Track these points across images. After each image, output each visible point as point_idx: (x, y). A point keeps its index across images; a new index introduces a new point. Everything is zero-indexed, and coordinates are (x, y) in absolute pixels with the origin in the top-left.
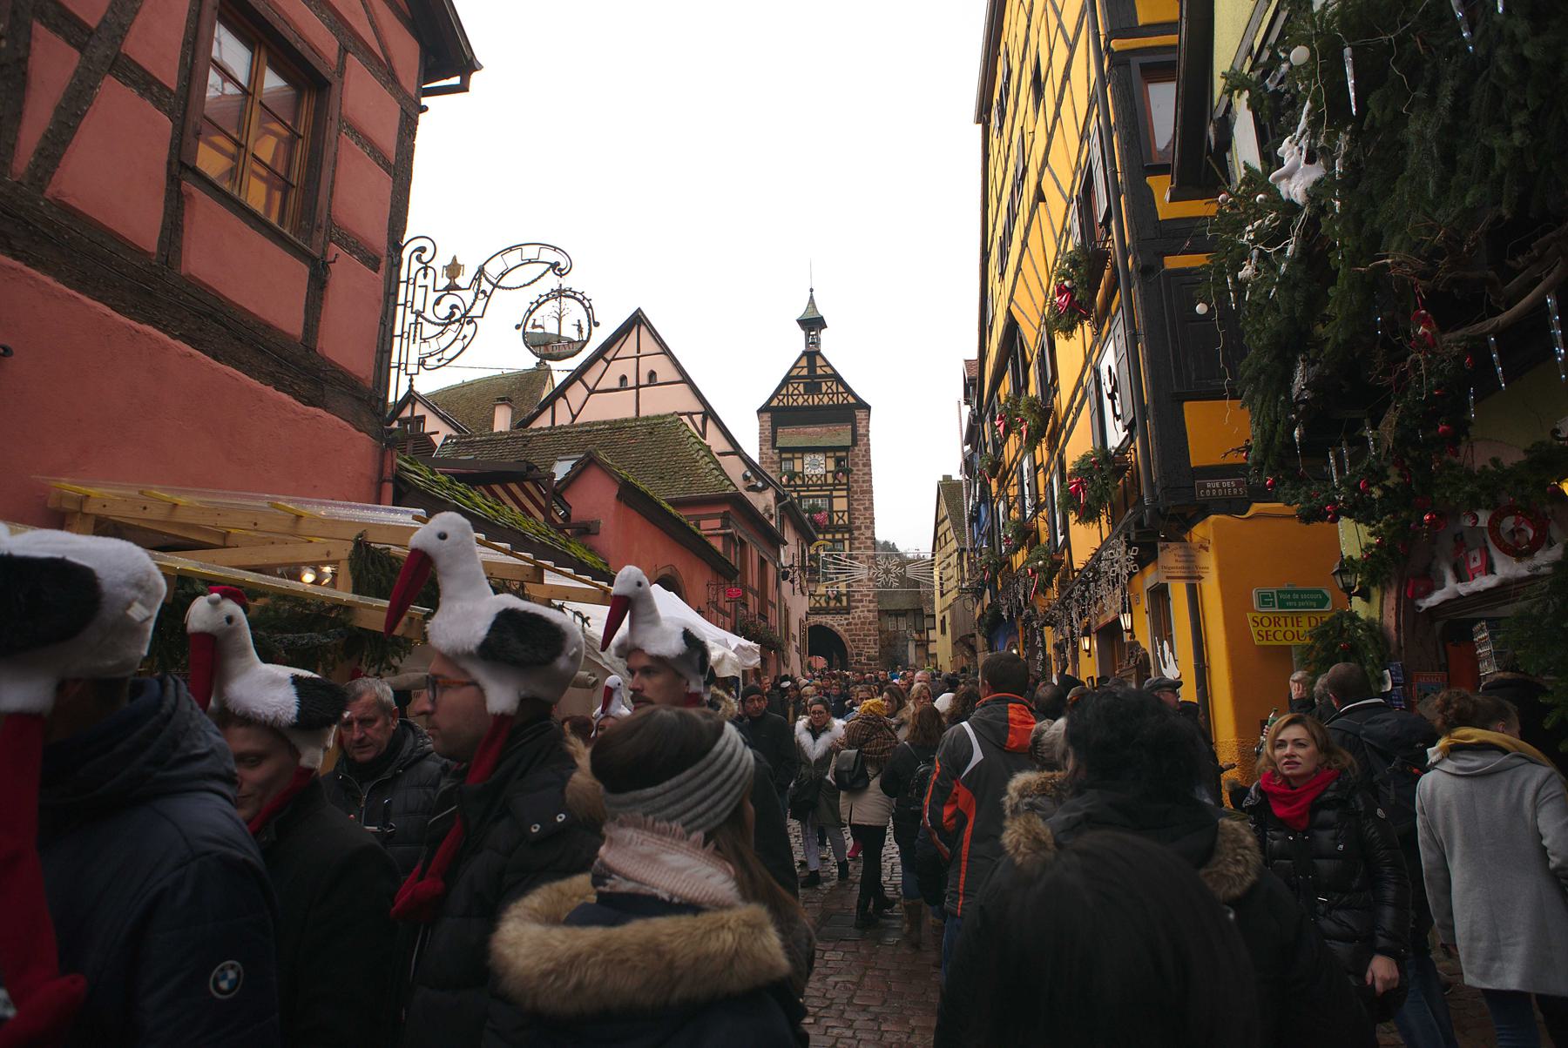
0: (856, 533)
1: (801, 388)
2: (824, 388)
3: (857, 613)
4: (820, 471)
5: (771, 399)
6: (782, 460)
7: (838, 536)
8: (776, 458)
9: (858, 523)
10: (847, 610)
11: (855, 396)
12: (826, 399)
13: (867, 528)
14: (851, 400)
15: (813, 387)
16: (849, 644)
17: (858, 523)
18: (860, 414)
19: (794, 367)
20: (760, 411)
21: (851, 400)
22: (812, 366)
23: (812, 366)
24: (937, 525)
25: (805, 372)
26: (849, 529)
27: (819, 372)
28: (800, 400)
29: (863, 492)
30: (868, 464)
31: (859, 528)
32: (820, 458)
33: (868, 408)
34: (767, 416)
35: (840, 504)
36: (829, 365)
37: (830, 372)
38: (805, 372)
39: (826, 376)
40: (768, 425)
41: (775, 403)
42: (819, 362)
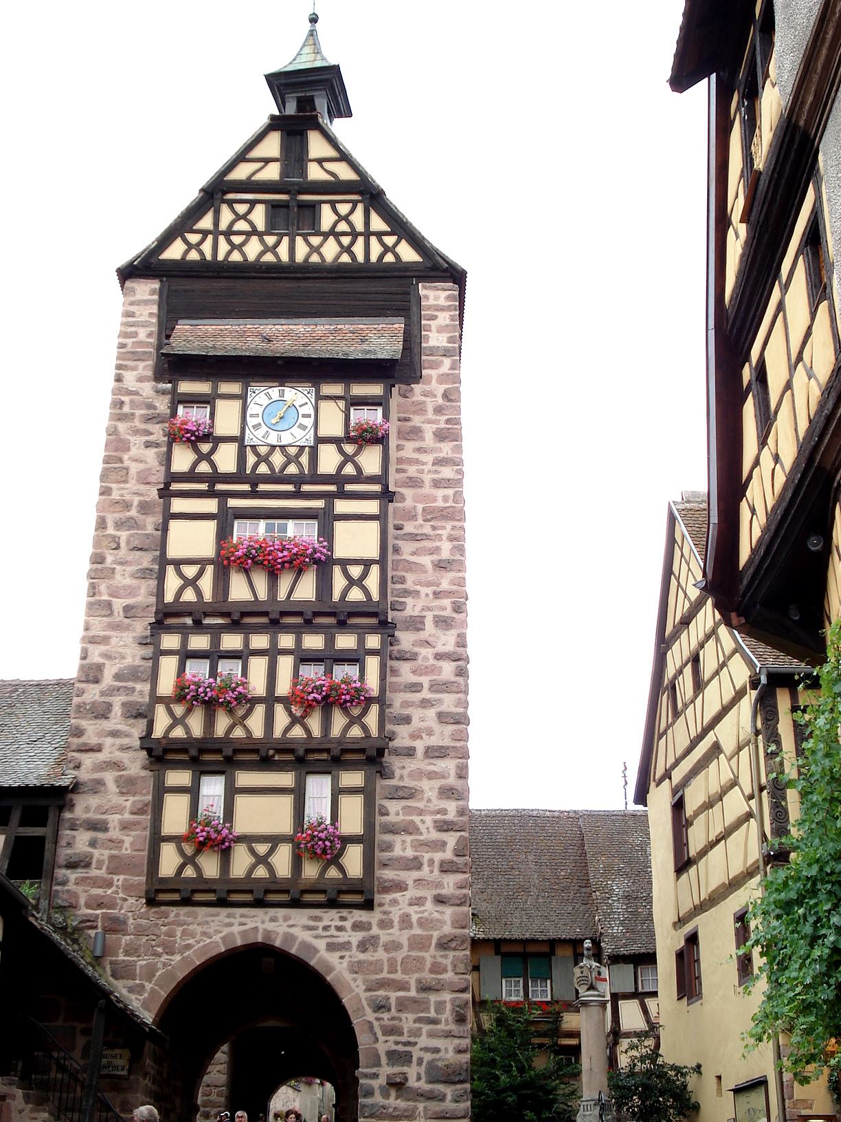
0: (406, 640)
1: (259, 216)
2: (327, 218)
3: (395, 905)
4: (298, 436)
5: (166, 240)
6: (181, 400)
7: (345, 641)
8: (162, 405)
10: (359, 896)
11: (417, 242)
12: (330, 250)
13: (443, 623)
14: (408, 254)
15: (294, 206)
16: (362, 1017)
17: (412, 607)
18: (434, 295)
19: (242, 157)
20: (128, 273)
21: (408, 254)
22: (294, 156)
23: (294, 156)
24: (664, 643)
25: (272, 173)
26: (378, 618)
28: (253, 249)
29: (434, 515)
30: (450, 434)
31: (416, 624)
32: (298, 396)
33: (456, 276)
34: (147, 289)
35: (356, 540)
36: (344, 157)
37: (345, 173)
39: (335, 187)
40: (148, 313)
41: (175, 251)
42: (317, 146)
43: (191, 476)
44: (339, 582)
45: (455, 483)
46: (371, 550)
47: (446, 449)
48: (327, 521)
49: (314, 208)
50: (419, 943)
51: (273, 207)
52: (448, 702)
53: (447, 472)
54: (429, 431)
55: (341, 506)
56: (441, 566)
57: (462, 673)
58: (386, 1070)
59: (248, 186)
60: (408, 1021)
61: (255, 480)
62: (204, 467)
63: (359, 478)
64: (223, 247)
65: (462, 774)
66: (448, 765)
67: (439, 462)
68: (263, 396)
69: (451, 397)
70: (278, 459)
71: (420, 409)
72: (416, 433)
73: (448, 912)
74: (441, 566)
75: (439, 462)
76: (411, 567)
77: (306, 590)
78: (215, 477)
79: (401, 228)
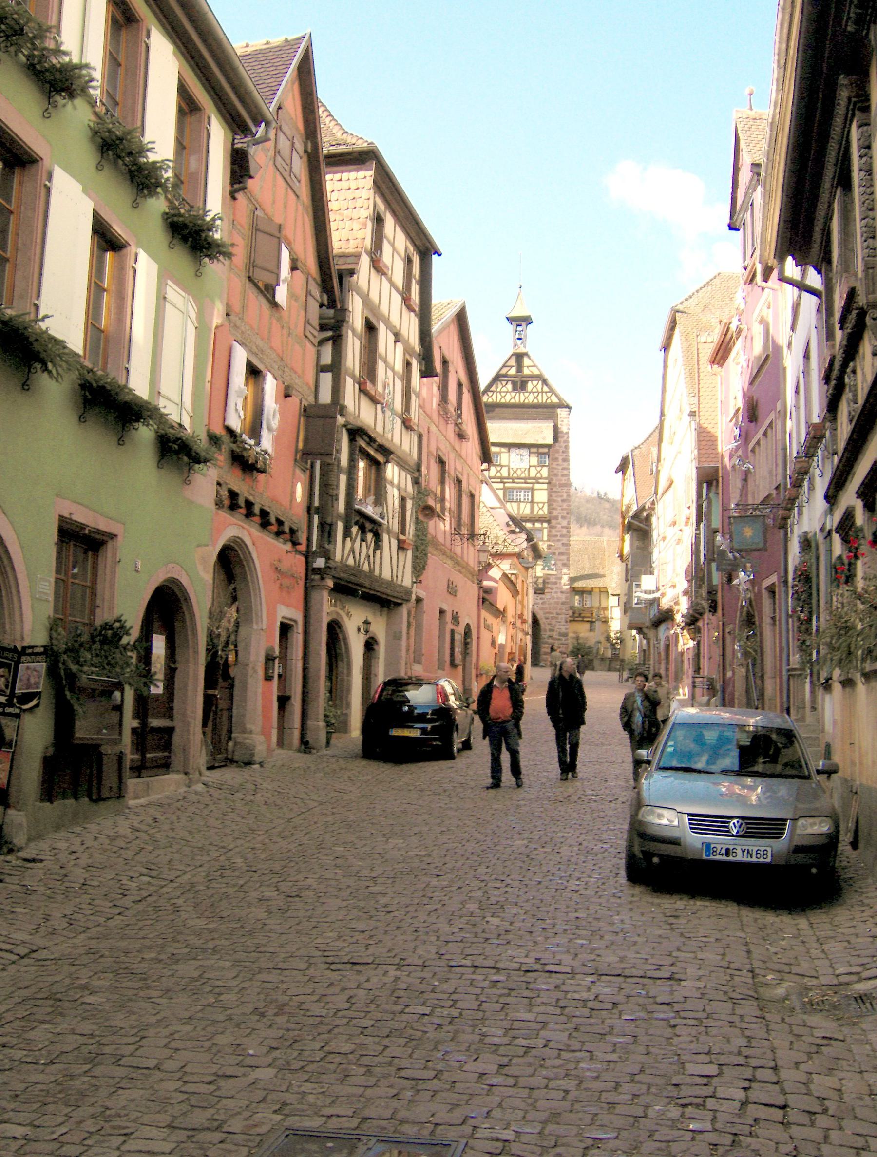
1: (509, 387)
2: (530, 386)
9: (555, 513)
13: (563, 518)
14: (555, 400)
15: (520, 385)
17: (555, 513)
18: (562, 413)
19: (504, 366)
23: (520, 368)
27: (526, 371)
29: (561, 485)
30: (566, 460)
31: (556, 518)
37: (536, 372)
38: (513, 371)
42: (526, 361)
43: (495, 478)
44: (536, 508)
45: (568, 475)
46: (545, 499)
47: (565, 465)
48: (533, 490)
49: (526, 382)
50: (557, 603)
51: (514, 384)
52: (565, 540)
53: (565, 472)
54: (560, 458)
55: (537, 486)
56: (563, 501)
57: (569, 532)
58: (548, 633)
59: (505, 376)
60: (553, 622)
61: (513, 479)
62: (499, 475)
63: (541, 478)
64: (499, 397)
65: (568, 560)
66: (564, 557)
67: (564, 469)
68: (514, 452)
69: (567, 447)
70: (519, 472)
71: (558, 451)
72: (556, 459)
73: (564, 596)
74: (563, 501)
75: (564, 469)
76: (555, 501)
77: (527, 512)
78: (502, 478)
79: (552, 391)
